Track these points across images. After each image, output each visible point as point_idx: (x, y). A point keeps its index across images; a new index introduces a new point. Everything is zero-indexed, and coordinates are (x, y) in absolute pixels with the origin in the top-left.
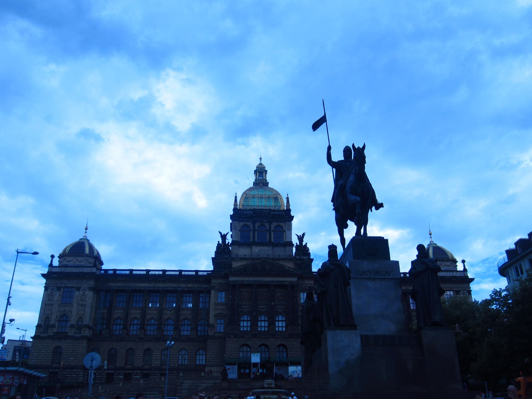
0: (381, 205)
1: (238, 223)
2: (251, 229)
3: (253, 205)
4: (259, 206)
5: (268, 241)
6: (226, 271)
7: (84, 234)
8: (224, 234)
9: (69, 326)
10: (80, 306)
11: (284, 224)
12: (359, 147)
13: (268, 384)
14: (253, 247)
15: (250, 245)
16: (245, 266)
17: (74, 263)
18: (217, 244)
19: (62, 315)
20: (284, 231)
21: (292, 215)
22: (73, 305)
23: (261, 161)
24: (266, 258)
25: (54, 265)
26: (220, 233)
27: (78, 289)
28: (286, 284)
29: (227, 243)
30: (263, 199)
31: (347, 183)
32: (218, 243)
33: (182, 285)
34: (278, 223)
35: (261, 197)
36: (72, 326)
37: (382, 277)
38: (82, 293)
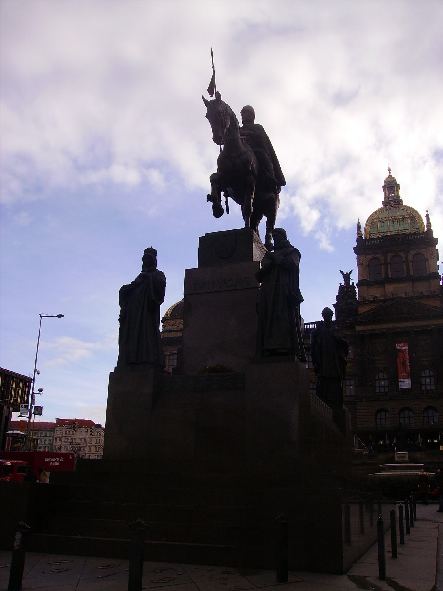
1: (364, 257)
2: (382, 262)
3: (383, 231)
4: (390, 232)
5: (406, 275)
6: (349, 319)
8: (347, 273)
11: (425, 250)
13: (399, 457)
14: (386, 285)
15: (382, 283)
16: (375, 310)
18: (339, 286)
20: (427, 260)
21: (435, 238)
23: (390, 173)
24: (401, 297)
26: (342, 272)
28: (430, 328)
29: (351, 284)
30: (395, 221)
32: (340, 285)
34: (418, 250)
35: (393, 220)
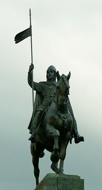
0: (82, 139)
12: (63, 75)
31: (47, 111)
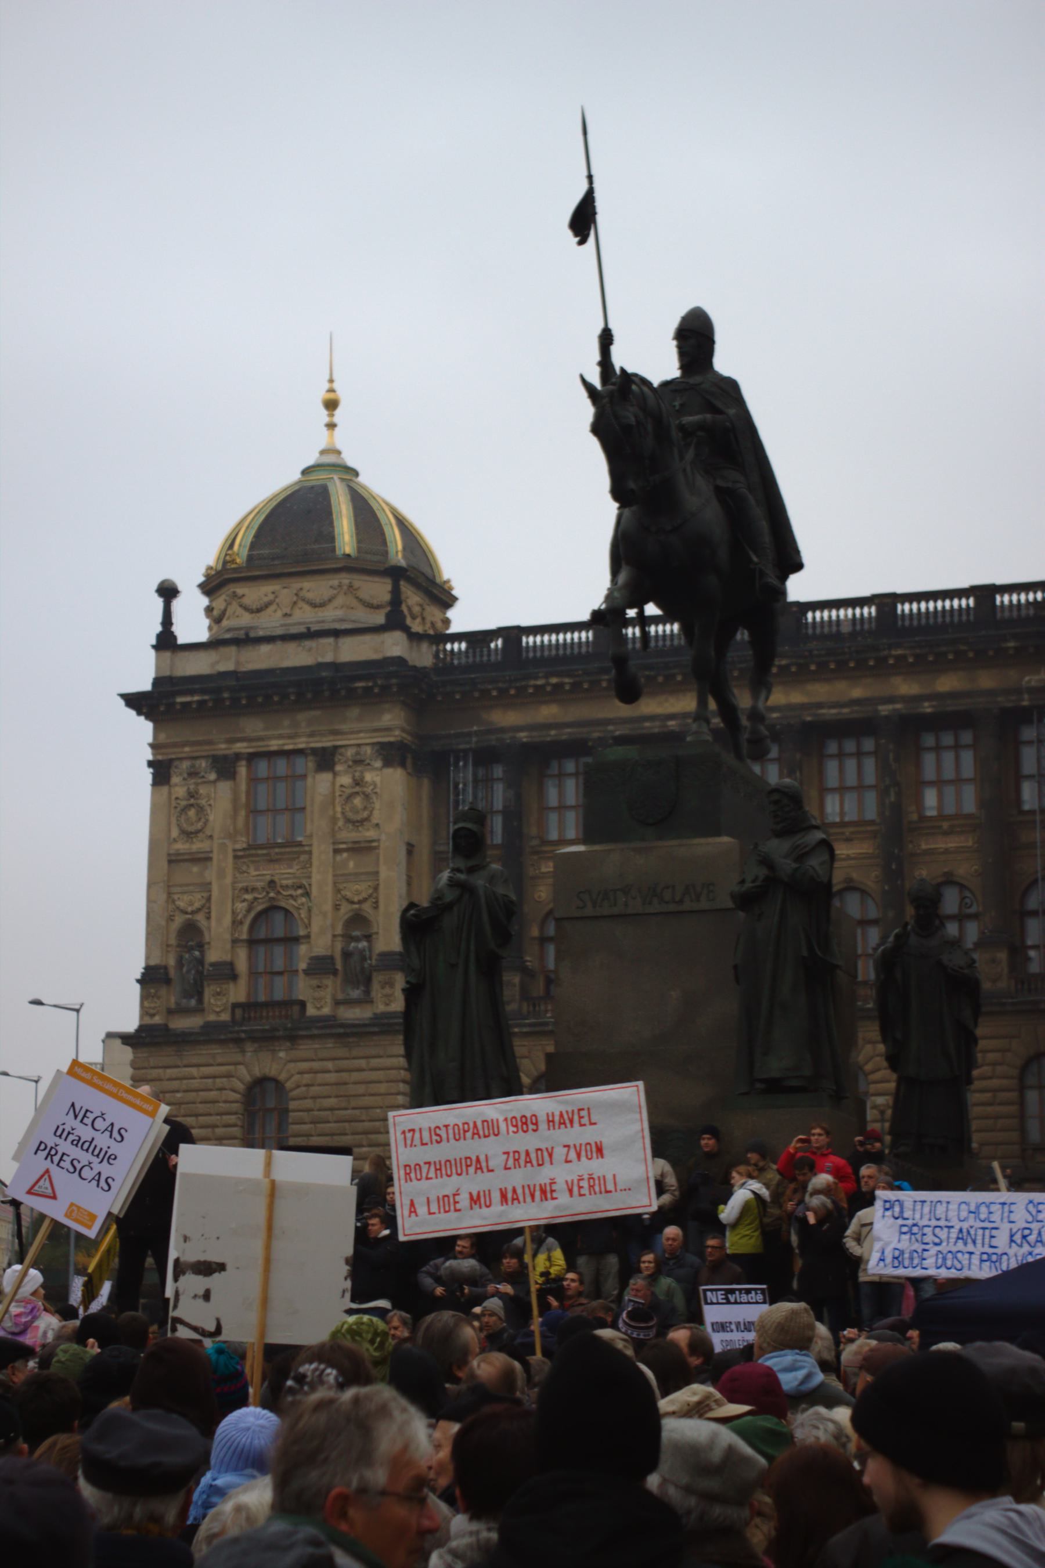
7: (321, 439)
9: (303, 965)
10: (345, 855)
17: (286, 615)
19: (260, 908)
22: (310, 853)
25: (181, 641)
27: (326, 760)
33: (906, 687)
36: (321, 966)
37: (672, 907)
38: (345, 780)
